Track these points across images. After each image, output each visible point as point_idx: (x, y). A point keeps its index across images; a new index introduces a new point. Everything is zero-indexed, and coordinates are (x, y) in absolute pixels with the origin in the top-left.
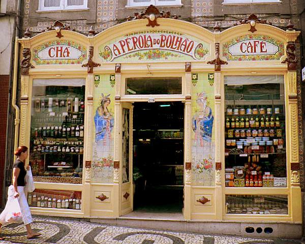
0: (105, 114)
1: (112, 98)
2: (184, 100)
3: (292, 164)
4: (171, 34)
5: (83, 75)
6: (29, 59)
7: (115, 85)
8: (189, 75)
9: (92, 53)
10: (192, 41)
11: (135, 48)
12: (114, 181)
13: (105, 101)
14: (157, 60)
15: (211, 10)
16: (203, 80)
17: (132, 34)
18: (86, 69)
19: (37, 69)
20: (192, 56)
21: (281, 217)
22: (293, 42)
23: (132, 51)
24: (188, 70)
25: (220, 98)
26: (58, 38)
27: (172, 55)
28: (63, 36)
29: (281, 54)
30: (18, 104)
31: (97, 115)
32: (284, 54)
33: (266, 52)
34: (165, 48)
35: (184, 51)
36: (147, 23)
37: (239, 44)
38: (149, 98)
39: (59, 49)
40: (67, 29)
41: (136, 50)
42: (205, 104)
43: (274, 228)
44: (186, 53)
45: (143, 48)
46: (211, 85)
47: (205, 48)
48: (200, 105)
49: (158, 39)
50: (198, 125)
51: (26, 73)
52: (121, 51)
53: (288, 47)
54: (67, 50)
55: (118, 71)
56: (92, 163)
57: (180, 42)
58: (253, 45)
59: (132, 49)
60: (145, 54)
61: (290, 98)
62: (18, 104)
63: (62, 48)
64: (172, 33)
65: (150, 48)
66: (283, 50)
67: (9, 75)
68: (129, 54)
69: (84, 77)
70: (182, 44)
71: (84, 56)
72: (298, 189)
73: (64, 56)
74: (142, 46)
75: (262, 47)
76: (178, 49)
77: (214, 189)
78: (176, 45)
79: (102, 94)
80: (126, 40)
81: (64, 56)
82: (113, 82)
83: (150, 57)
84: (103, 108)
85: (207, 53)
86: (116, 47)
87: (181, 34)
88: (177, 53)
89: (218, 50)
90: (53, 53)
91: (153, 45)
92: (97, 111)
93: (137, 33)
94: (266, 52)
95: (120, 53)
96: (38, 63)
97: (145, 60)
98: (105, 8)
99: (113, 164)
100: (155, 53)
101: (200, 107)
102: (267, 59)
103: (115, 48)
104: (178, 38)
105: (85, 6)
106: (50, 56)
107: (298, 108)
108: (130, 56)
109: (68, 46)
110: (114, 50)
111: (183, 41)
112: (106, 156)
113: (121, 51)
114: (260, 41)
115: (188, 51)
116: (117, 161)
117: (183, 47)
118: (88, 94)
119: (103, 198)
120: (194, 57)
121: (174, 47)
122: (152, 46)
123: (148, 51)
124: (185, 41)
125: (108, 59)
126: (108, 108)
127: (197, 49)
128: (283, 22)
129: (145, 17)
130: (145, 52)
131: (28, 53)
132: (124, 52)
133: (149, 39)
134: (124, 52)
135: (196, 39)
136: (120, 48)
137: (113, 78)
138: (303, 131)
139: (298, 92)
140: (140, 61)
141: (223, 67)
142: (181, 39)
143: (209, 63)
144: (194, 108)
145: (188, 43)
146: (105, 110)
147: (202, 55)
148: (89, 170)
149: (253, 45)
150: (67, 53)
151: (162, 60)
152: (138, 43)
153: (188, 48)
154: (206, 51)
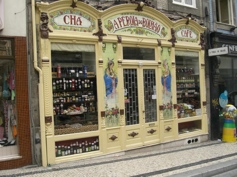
0: (111, 74)
1: (115, 62)
2: (158, 64)
3: (203, 102)
4: (148, 18)
5: (93, 41)
6: (47, 23)
7: (117, 52)
9: (100, 24)
10: (159, 25)
11: (128, 25)
13: (111, 64)
14: (141, 36)
16: (166, 50)
17: (126, 14)
18: (97, 37)
19: (55, 33)
23: (150, 29)
26: (71, 8)
27: (150, 33)
28: (76, 7)
29: (198, 40)
34: (145, 27)
35: (155, 31)
36: (136, 8)
38: (139, 62)
39: (73, 17)
42: (167, 68)
43: (199, 138)
45: (133, 26)
48: (164, 68)
49: (141, 21)
50: (165, 80)
51: (46, 37)
54: (80, 19)
57: (153, 24)
58: (187, 33)
60: (135, 30)
61: (202, 65)
63: (75, 17)
64: (149, 17)
65: (137, 26)
67: (26, 37)
69: (94, 43)
70: (154, 26)
71: (93, 26)
73: (78, 25)
74: (132, 24)
75: (190, 34)
78: (151, 26)
79: (108, 58)
81: (78, 25)
82: (115, 49)
83: (137, 33)
84: (110, 69)
87: (153, 19)
88: (152, 32)
90: (68, 20)
91: (139, 24)
92: (105, 72)
93: (128, 14)
94: (192, 37)
95: (118, 28)
96: (55, 28)
97: (134, 34)
99: (119, 111)
100: (140, 30)
103: (115, 23)
104: (152, 21)
108: (125, 31)
109: (80, 16)
110: (115, 24)
111: (155, 24)
114: (190, 31)
117: (155, 28)
118: (98, 58)
119: (113, 138)
120: (161, 36)
121: (150, 27)
122: (138, 25)
123: (136, 28)
124: (156, 24)
125: (111, 31)
126: (112, 69)
127: (162, 31)
129: (138, 3)
130: (134, 28)
131: (44, 18)
132: (121, 27)
133: (136, 20)
134: (121, 27)
136: (118, 23)
137: (115, 46)
142: (154, 22)
143: (169, 41)
145: (157, 26)
146: (111, 71)
149: (187, 33)
150: (79, 22)
151: (144, 36)
153: (157, 30)
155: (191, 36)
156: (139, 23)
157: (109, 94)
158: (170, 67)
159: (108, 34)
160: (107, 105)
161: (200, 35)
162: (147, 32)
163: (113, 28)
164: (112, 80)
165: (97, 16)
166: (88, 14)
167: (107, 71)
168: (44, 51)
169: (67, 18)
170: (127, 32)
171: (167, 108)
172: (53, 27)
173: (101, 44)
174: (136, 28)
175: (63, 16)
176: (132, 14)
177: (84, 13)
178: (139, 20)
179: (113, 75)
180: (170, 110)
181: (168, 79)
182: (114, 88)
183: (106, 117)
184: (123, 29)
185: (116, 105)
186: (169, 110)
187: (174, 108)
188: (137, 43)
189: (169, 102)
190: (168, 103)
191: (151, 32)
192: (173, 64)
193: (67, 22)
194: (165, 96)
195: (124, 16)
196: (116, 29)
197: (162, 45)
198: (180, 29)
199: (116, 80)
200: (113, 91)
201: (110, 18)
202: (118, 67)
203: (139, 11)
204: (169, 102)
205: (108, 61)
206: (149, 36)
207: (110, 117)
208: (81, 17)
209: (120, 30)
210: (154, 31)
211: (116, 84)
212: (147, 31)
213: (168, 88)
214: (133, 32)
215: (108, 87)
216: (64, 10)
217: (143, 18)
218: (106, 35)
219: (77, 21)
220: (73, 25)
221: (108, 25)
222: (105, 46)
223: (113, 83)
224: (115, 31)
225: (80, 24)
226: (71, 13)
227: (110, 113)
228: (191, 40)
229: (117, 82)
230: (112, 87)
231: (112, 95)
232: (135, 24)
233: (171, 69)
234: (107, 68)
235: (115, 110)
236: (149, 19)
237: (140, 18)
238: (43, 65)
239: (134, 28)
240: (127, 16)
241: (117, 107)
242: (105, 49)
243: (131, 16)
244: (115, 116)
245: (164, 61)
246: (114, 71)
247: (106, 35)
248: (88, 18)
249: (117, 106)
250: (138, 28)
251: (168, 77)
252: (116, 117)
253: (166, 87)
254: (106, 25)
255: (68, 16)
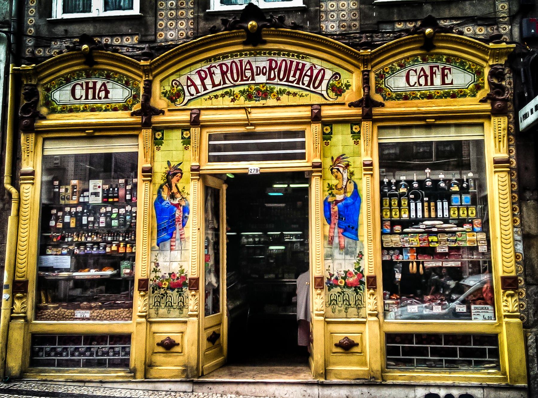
0: (173, 196)
1: (186, 168)
2: (311, 169)
3: (504, 279)
7: (190, 147)
8: (317, 127)
11: (225, 83)
12: (190, 313)
13: (175, 174)
15: (354, 15)
17: (219, 59)
20: (322, 95)
21: (489, 373)
22: (501, 65)
24: (316, 118)
25: (371, 165)
27: (289, 93)
28: (97, 63)
29: (478, 87)
30: (15, 183)
31: (160, 199)
32: (483, 87)
33: (452, 83)
35: (308, 86)
37: (404, 73)
39: (91, 85)
40: (103, 49)
41: (225, 86)
42: (346, 176)
44: (312, 89)
45: (238, 83)
46: (357, 143)
47: (344, 81)
48: (336, 177)
49: (264, 67)
51: (30, 129)
52: (200, 88)
53: (492, 74)
55: (195, 122)
56: (151, 283)
57: (302, 70)
58: (428, 73)
59: (219, 85)
60: (242, 92)
61: (496, 162)
62: (15, 183)
63: (95, 83)
64: (288, 55)
66: (483, 80)
68: (215, 93)
70: (305, 75)
72: (518, 324)
74: (236, 79)
75: (444, 76)
76: (298, 83)
77: (364, 323)
78: (294, 76)
79: (168, 162)
80: (209, 69)
81: (100, 98)
82: (186, 142)
83: (249, 97)
85: (347, 88)
86: (192, 81)
87: (303, 58)
89: (366, 81)
90: (80, 92)
91: (256, 77)
92: (159, 193)
93: (227, 57)
95: (198, 92)
96: (53, 111)
97: (242, 101)
98: (171, 14)
99: (187, 282)
100: (258, 90)
101: (337, 182)
102: (454, 96)
103: (189, 83)
104: (298, 64)
105: (136, 11)
106: (75, 99)
107: (511, 180)
108: (216, 97)
110: (188, 86)
111: (306, 68)
112: (175, 268)
113: (200, 88)
114: (441, 67)
115: (316, 86)
116: (196, 276)
117: (307, 79)
118: (142, 164)
121: (291, 79)
122: (253, 79)
123: (246, 87)
124: (311, 69)
126: (178, 185)
127: (331, 82)
128: (482, 31)
130: (242, 88)
131: (33, 93)
133: (248, 67)
134: (205, 89)
135: (330, 66)
136: (198, 82)
138: (521, 221)
139: (509, 152)
140: (232, 105)
141: (376, 111)
142: (304, 65)
143: (351, 105)
144: (327, 182)
145: (315, 72)
146: (174, 190)
147: (339, 91)
148: (143, 296)
149: (428, 73)
151: (271, 101)
152: (229, 75)
154: (346, 85)
155: (447, 81)
156: (257, 75)
157: (164, 240)
158: (355, 173)
159: (169, 110)
160: (157, 265)
161: (487, 71)
162: (281, 92)
163: (184, 94)
164: (175, 209)
165: (141, 74)
166: (124, 75)
167: (163, 189)
168: (26, 156)
169: (78, 88)
170: (220, 99)
171: (343, 284)
172: (49, 109)
173: (147, 133)
174: (246, 87)
175: (69, 88)
176: (236, 56)
177: (116, 73)
178: (257, 67)
179: (178, 199)
180: (355, 290)
181: (346, 206)
182: (178, 227)
183: (153, 292)
184: (210, 94)
185: (181, 267)
186: (350, 292)
187: (368, 288)
188: (247, 122)
189: (352, 269)
190: (346, 272)
191: (292, 90)
192: (368, 166)
193: (78, 96)
194: (336, 253)
195: (213, 65)
196: (192, 95)
197: (323, 119)
198: (400, 65)
199: (186, 210)
200: (177, 235)
201: (178, 73)
202: (192, 179)
203: (255, 45)
204: (352, 269)
205: (168, 169)
206: (285, 99)
207: (162, 294)
208: (108, 82)
209: (203, 98)
210: (304, 87)
211: (185, 219)
212: (280, 89)
213: (345, 230)
214: (237, 96)
215: (165, 224)
216: (73, 72)
217: (271, 61)
218: (162, 112)
219: (100, 91)
220: (90, 100)
221: (170, 91)
222: (161, 136)
223: (177, 215)
224: (189, 100)
225: (106, 97)
226: (88, 76)
227: (165, 284)
228: (446, 93)
229: (186, 215)
230: (174, 224)
231: (173, 244)
232: (244, 78)
233: (361, 179)
234: (165, 183)
235: (178, 278)
236: (288, 59)
237: (262, 62)
238: (22, 182)
239: (242, 88)
240: (224, 62)
241: (182, 271)
242: (161, 144)
243: (233, 62)
244: (178, 292)
245: (334, 160)
246: (180, 190)
247: (162, 112)
248: (124, 82)
249: (183, 270)
250: (253, 87)
251: (350, 201)
252: (180, 295)
253: (339, 227)
254: (167, 92)
255: (80, 83)
